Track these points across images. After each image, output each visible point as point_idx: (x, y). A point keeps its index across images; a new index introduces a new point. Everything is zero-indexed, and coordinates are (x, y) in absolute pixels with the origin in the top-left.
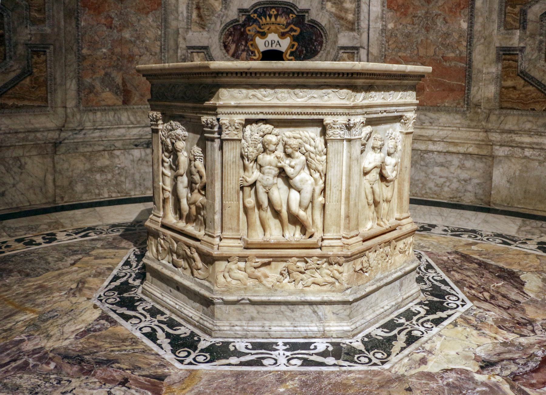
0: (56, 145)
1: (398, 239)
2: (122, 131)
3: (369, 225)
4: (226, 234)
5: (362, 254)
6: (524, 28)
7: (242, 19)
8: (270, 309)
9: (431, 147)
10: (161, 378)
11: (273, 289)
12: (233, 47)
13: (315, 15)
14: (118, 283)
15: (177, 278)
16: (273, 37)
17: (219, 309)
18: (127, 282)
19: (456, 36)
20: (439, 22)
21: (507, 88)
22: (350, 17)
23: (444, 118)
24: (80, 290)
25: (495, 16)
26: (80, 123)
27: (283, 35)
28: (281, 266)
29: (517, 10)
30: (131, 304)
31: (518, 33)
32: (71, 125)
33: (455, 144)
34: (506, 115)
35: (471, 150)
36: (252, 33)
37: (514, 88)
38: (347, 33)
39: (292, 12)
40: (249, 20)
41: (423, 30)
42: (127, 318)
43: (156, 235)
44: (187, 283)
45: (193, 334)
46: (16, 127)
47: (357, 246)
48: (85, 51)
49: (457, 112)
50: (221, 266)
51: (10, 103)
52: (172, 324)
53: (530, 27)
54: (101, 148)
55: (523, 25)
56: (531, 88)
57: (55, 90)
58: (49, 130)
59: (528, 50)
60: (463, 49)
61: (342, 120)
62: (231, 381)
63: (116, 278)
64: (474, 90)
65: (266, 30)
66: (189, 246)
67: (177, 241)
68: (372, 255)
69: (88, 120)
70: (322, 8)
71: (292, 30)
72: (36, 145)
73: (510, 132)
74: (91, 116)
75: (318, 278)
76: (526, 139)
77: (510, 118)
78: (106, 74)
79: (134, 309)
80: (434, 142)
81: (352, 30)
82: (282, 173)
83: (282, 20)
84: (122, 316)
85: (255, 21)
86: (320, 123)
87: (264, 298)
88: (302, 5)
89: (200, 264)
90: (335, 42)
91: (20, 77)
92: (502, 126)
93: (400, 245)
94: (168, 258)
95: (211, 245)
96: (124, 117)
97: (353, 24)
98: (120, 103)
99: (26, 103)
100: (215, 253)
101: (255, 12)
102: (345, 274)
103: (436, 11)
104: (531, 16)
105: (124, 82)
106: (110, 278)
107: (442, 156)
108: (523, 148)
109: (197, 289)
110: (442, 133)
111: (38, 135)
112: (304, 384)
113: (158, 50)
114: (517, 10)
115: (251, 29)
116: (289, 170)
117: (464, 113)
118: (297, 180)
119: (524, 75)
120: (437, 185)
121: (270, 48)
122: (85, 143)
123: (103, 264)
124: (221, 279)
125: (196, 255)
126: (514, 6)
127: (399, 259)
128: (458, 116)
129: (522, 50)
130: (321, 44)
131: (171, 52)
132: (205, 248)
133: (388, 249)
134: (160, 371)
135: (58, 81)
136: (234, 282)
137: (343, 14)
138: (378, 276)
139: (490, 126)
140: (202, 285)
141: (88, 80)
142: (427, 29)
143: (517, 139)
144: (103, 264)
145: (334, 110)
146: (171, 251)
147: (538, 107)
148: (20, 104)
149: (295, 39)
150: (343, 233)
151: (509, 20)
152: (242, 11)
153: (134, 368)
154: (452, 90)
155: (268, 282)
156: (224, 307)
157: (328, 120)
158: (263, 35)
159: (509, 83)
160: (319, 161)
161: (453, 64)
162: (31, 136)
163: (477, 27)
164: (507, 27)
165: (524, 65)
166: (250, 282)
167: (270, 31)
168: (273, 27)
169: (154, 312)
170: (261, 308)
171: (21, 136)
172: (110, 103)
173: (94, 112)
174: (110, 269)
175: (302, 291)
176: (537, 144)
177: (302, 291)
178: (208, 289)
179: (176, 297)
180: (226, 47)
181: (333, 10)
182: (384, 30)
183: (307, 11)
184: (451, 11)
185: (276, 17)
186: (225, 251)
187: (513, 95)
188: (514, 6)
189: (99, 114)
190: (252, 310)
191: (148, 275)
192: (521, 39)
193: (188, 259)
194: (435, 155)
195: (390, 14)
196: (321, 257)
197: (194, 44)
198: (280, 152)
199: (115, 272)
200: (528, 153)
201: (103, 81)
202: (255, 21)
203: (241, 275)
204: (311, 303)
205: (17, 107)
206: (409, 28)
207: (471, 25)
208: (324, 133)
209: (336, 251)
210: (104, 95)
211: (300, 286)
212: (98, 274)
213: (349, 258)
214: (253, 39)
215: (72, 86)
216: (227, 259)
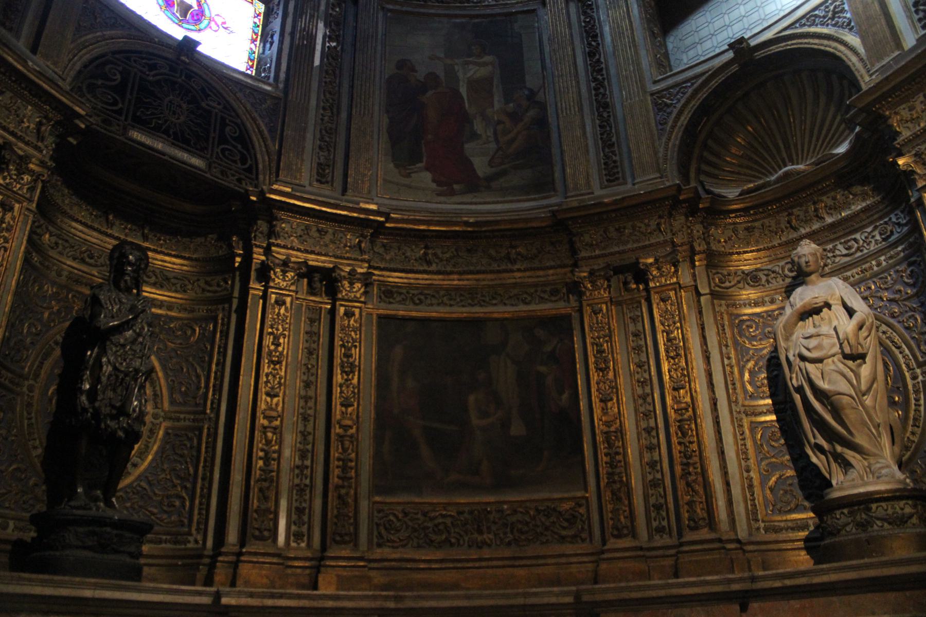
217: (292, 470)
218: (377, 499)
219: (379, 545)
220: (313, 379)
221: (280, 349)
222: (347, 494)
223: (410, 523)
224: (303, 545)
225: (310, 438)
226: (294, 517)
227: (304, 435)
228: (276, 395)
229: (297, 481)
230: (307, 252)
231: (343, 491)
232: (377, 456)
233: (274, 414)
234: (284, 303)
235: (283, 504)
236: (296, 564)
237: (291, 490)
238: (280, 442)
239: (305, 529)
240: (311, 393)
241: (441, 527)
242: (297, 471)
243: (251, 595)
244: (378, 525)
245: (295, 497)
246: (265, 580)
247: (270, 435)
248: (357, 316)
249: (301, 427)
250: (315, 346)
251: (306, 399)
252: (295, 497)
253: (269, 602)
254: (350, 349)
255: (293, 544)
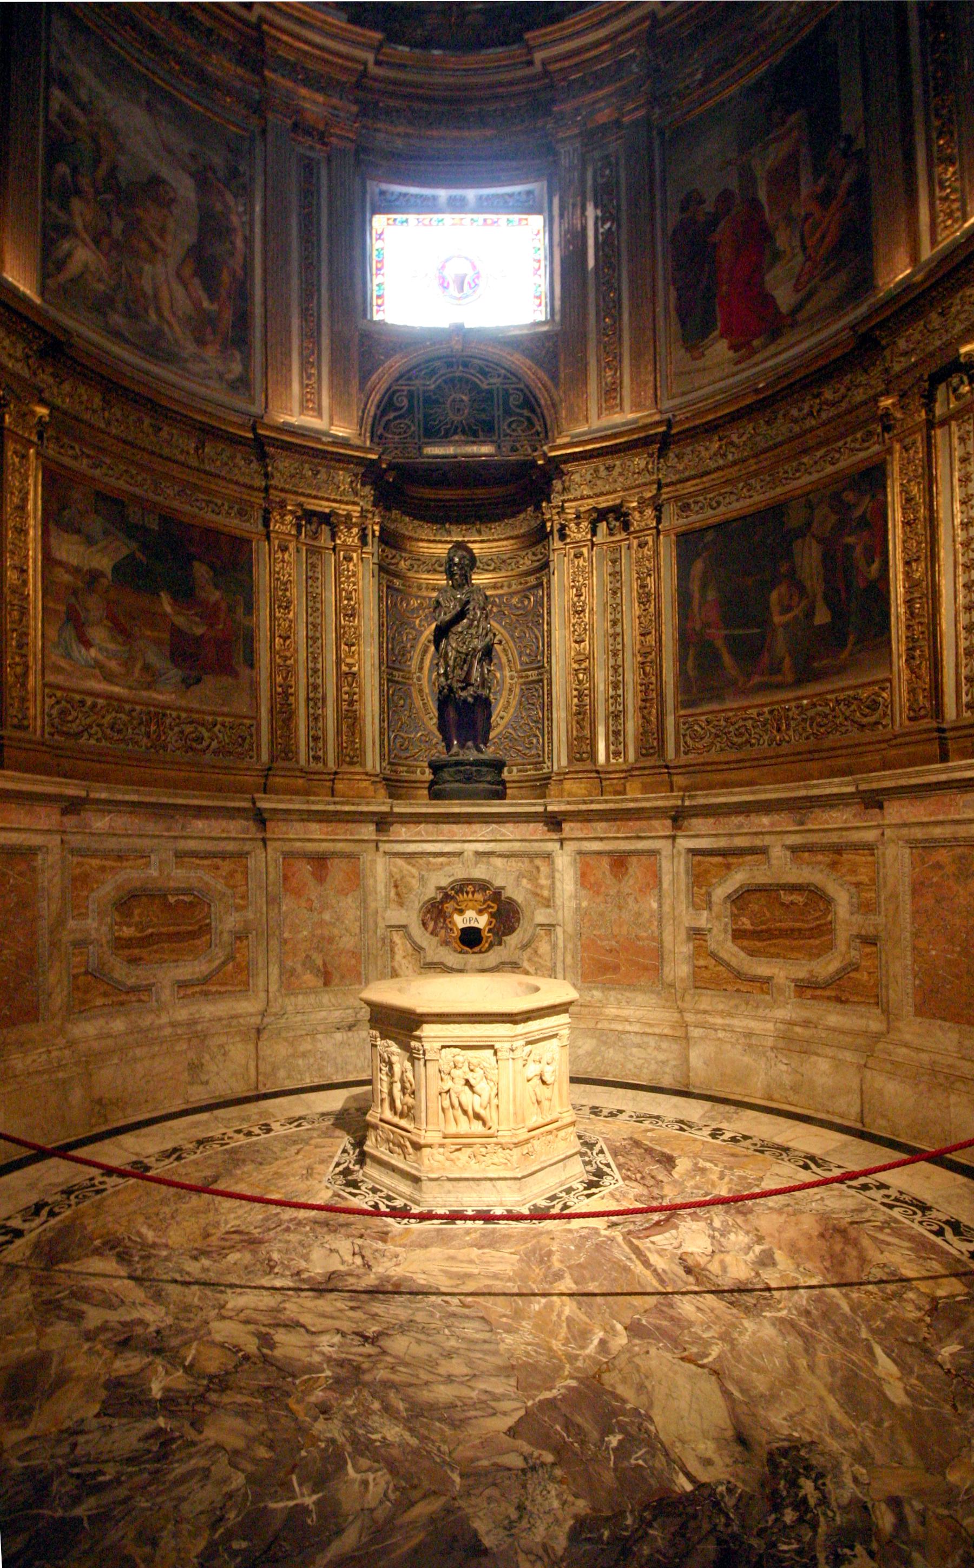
0: (259, 1031)
1: (558, 1129)
2: (324, 1014)
3: (534, 1118)
4: (430, 1127)
5: (527, 1141)
6: (710, 909)
7: (440, 896)
8: (462, 1184)
9: (628, 1028)
10: (386, 1233)
11: (464, 1168)
12: (431, 925)
13: (510, 892)
14: (341, 1168)
15: (393, 1162)
16: (470, 914)
17: (426, 1185)
18: (347, 1168)
19: (647, 916)
20: (631, 900)
21: (700, 968)
22: (546, 893)
23: (640, 998)
24: (311, 1175)
25: (682, 897)
26: (282, 1007)
27: (480, 912)
28: (469, 1151)
29: (703, 890)
30: (355, 1184)
31: (705, 913)
32: (273, 1010)
33: (651, 1025)
34: (700, 995)
35: (666, 1031)
36: (450, 910)
37: (706, 967)
38: (543, 910)
39: (488, 889)
40: (447, 897)
41: (616, 909)
42: (354, 1195)
43: (375, 1127)
44: (401, 1165)
45: (406, 1205)
46: (219, 1013)
47: (526, 1136)
48: (286, 935)
49: (653, 992)
50: (426, 1151)
51: (214, 989)
52: (389, 1198)
53: (715, 908)
54: (303, 1032)
55: (709, 906)
56: (721, 968)
57: (257, 974)
58: (251, 1015)
59: (715, 931)
60: (654, 928)
61: (508, 1045)
62: (434, 1234)
63: (338, 1165)
64: (666, 970)
65: (463, 907)
66: (403, 1137)
67: (393, 1132)
68: (535, 1142)
69: (290, 1003)
70: (518, 885)
71: (489, 907)
72: (240, 1032)
73: (705, 1012)
74: (292, 998)
75: (496, 1161)
76: (719, 1021)
77: (704, 998)
78: (307, 956)
79: (359, 1188)
80: (630, 1023)
81: (548, 906)
82: (467, 1083)
83: (479, 896)
84: (350, 1193)
85: (453, 898)
86: (492, 1047)
87: (457, 1176)
88: (498, 882)
89: (411, 1150)
90: (532, 919)
91: (224, 963)
92: (697, 1006)
93: (562, 1133)
94: (386, 1146)
95: (419, 1136)
96: (326, 999)
97: (549, 900)
98: (320, 983)
99: (229, 988)
100: (422, 1142)
101: (452, 889)
102: (515, 1157)
103: (627, 890)
104: (715, 899)
105: (325, 964)
106: (333, 1164)
107: (639, 1037)
108: (716, 1030)
109: (408, 1169)
110: (639, 1013)
111: (241, 1020)
112: (483, 1235)
113: (358, 931)
114: (703, 890)
115: (449, 906)
116: (472, 1082)
117: (658, 993)
118: (477, 1089)
119: (713, 955)
120: (636, 1067)
121: (468, 925)
122: (287, 1028)
123: (324, 1153)
124: (426, 1162)
125: (408, 1144)
126: (700, 888)
127: (562, 1144)
128: (653, 996)
129: (710, 930)
130: (518, 920)
131: (371, 933)
132: (414, 1138)
133: (550, 1137)
134: (385, 1229)
135: (260, 965)
136: (436, 1164)
137: (539, 891)
138: (543, 1158)
139: (685, 1005)
140: (412, 1167)
141: (289, 963)
142: (620, 908)
143: (711, 1020)
144: (324, 1153)
145: (501, 1038)
146: (388, 1141)
147: (729, 988)
148: (223, 989)
149: (492, 915)
150: (512, 1125)
151: (696, 900)
152: (439, 888)
153: (366, 1228)
154: (646, 968)
155: (459, 1164)
156: (429, 1183)
157: (497, 1046)
158: (461, 912)
159: (702, 962)
160: (492, 1074)
161: (646, 943)
162: (234, 1022)
163: (666, 908)
164: (695, 906)
165: (712, 945)
166: (448, 1163)
167: (467, 908)
168: (470, 904)
169: (374, 1190)
170: (455, 1183)
171: (224, 1022)
172: (311, 985)
173: (296, 995)
174: (332, 1157)
175: (484, 1170)
176: (729, 1025)
177: (484, 1170)
178: (416, 1169)
179: (392, 1178)
180: (424, 924)
181: (529, 886)
182: (578, 908)
183: (503, 888)
184: (640, 891)
185: (473, 893)
186: (429, 1141)
187: (706, 974)
188: (700, 888)
189: (300, 997)
190: (448, 1185)
191: (368, 1161)
192: (708, 920)
193: (401, 1146)
194: (632, 1036)
195: (584, 892)
196: (497, 1144)
197: (393, 922)
198: (466, 1068)
199: (336, 1159)
200: (721, 1034)
201: (304, 965)
202: (453, 898)
203: (441, 1158)
204: (491, 1179)
205: (220, 993)
206: (602, 906)
207: (660, 906)
208: (495, 1053)
209: (507, 1140)
210: (305, 977)
211: (483, 1165)
212: (322, 1162)
213: (517, 1145)
214: (451, 916)
215: (274, 970)
216: (430, 1146)
217: (607, 700)
218: (682, 712)
219: (686, 753)
220: (619, 616)
221: (582, 598)
222: (650, 713)
223: (713, 730)
224: (621, 760)
225: (620, 670)
226: (612, 739)
227: (615, 669)
228: (583, 641)
229: (612, 709)
230: (597, 495)
231: (646, 711)
232: (682, 674)
233: (582, 657)
234: (582, 554)
235: (601, 730)
236: (612, 776)
237: (607, 718)
238: (591, 678)
239: (621, 747)
240: (619, 630)
241: (742, 730)
242: (611, 701)
243: (569, 803)
244: (684, 736)
245: (611, 722)
246: (584, 791)
247: (581, 676)
248: (651, 543)
249: (611, 662)
250: (618, 585)
251: (615, 635)
252: (611, 722)
253: (583, 807)
254: (645, 579)
255: (613, 761)
